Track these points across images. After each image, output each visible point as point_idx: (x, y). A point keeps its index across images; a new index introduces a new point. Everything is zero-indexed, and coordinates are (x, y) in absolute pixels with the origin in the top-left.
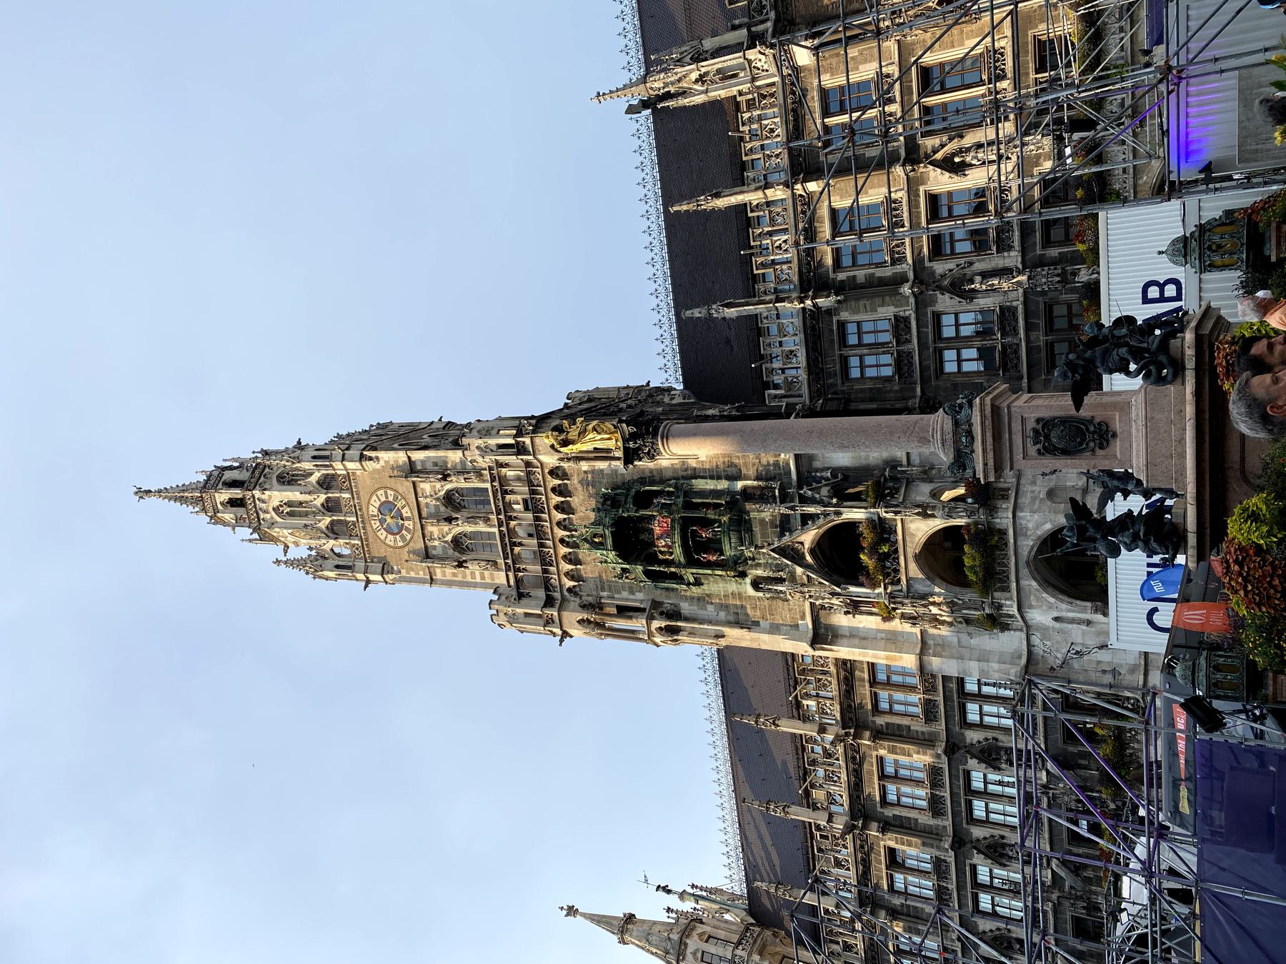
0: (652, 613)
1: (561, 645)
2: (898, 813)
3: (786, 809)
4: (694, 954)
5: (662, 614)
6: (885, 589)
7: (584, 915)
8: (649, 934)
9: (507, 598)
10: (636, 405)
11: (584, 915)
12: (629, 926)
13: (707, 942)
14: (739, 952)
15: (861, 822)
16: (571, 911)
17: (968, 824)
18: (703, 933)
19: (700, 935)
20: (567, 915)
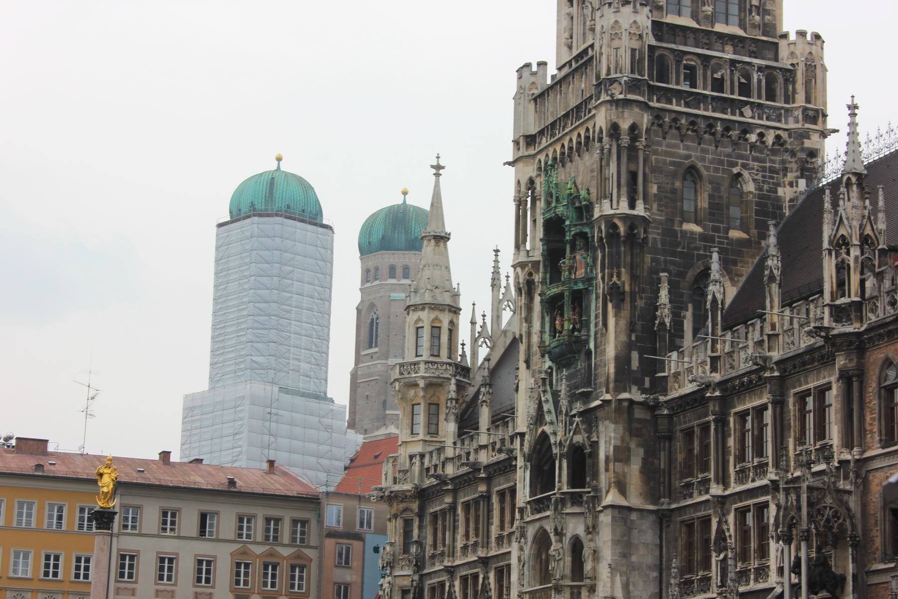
0: (527, 265)
1: (505, 164)
2: (495, 507)
3: (484, 404)
4: (419, 320)
5: (530, 274)
6: (529, 502)
7: (437, 185)
8: (429, 266)
9: (533, 83)
10: (767, 146)
11: (437, 185)
12: (433, 241)
13: (433, 327)
14: (422, 366)
15: (483, 475)
16: (438, 167)
17: (496, 568)
18: (440, 321)
19: (436, 319)
20: (433, 167)
